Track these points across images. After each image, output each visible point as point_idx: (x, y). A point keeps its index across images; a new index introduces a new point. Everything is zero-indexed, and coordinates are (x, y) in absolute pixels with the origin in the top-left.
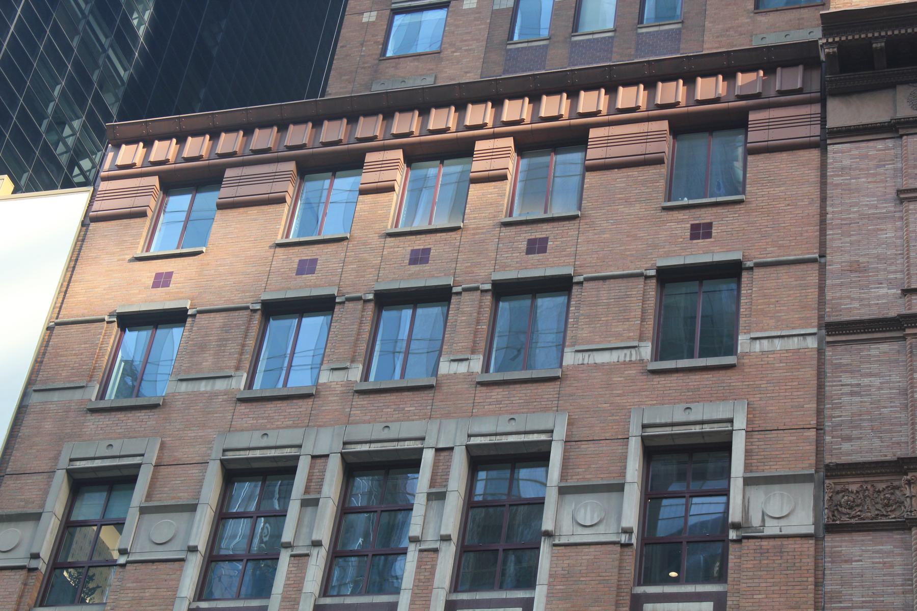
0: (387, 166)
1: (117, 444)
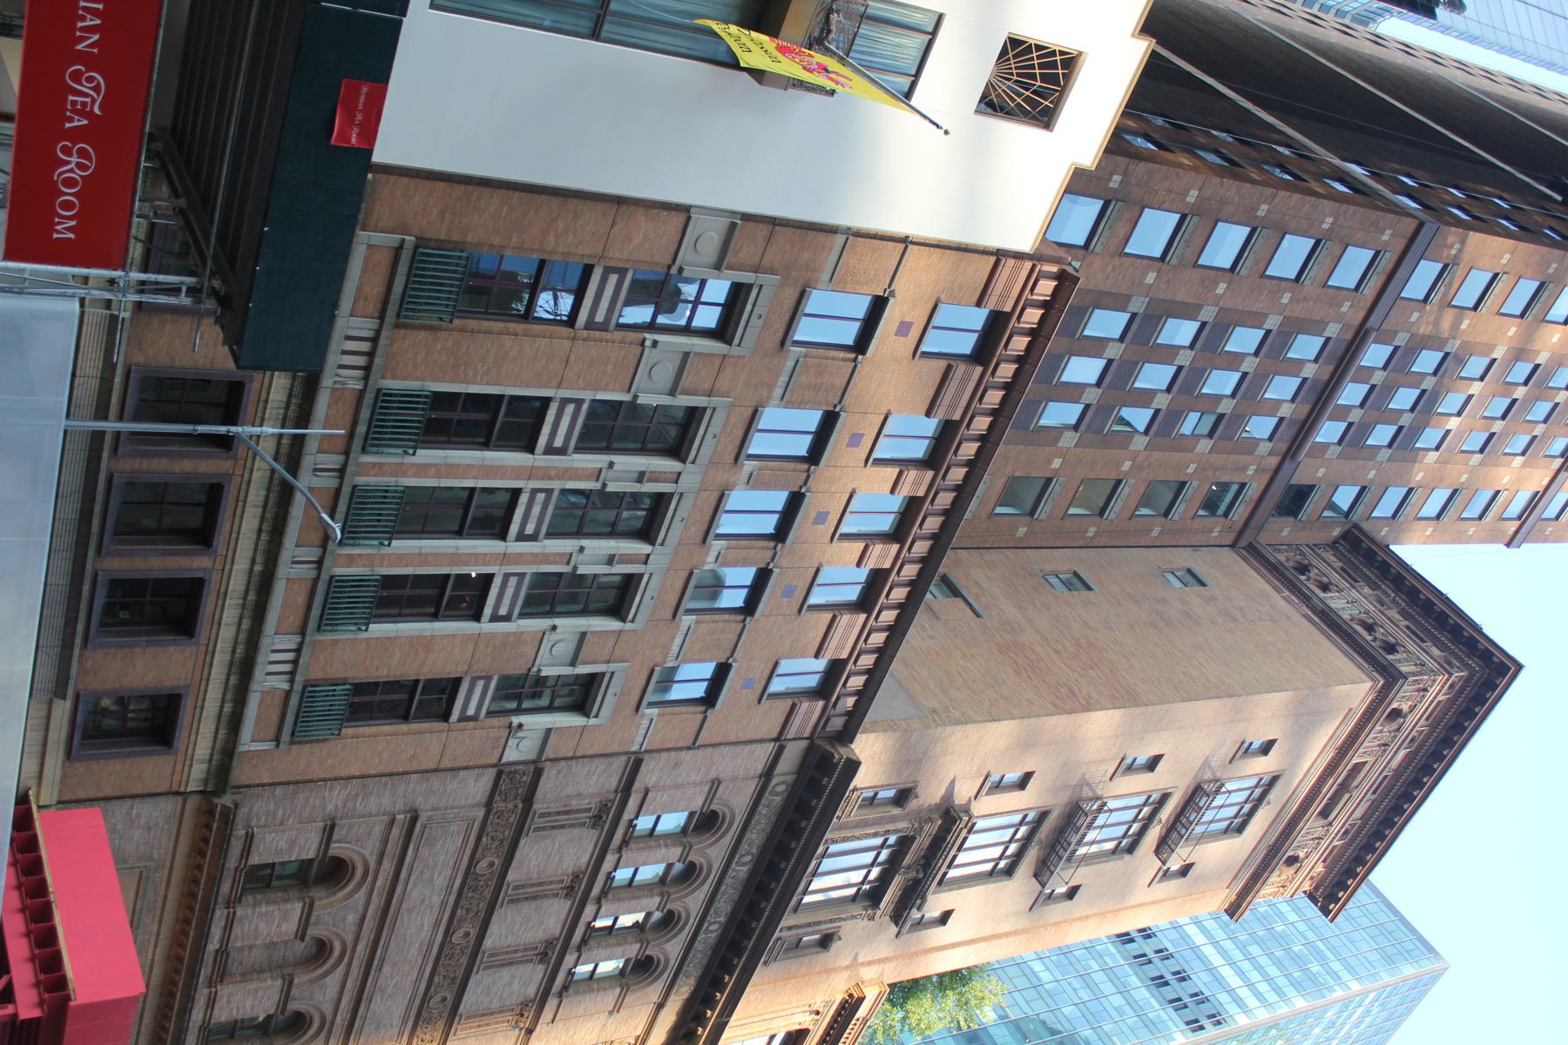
0: (882, 556)
1: (760, 322)
